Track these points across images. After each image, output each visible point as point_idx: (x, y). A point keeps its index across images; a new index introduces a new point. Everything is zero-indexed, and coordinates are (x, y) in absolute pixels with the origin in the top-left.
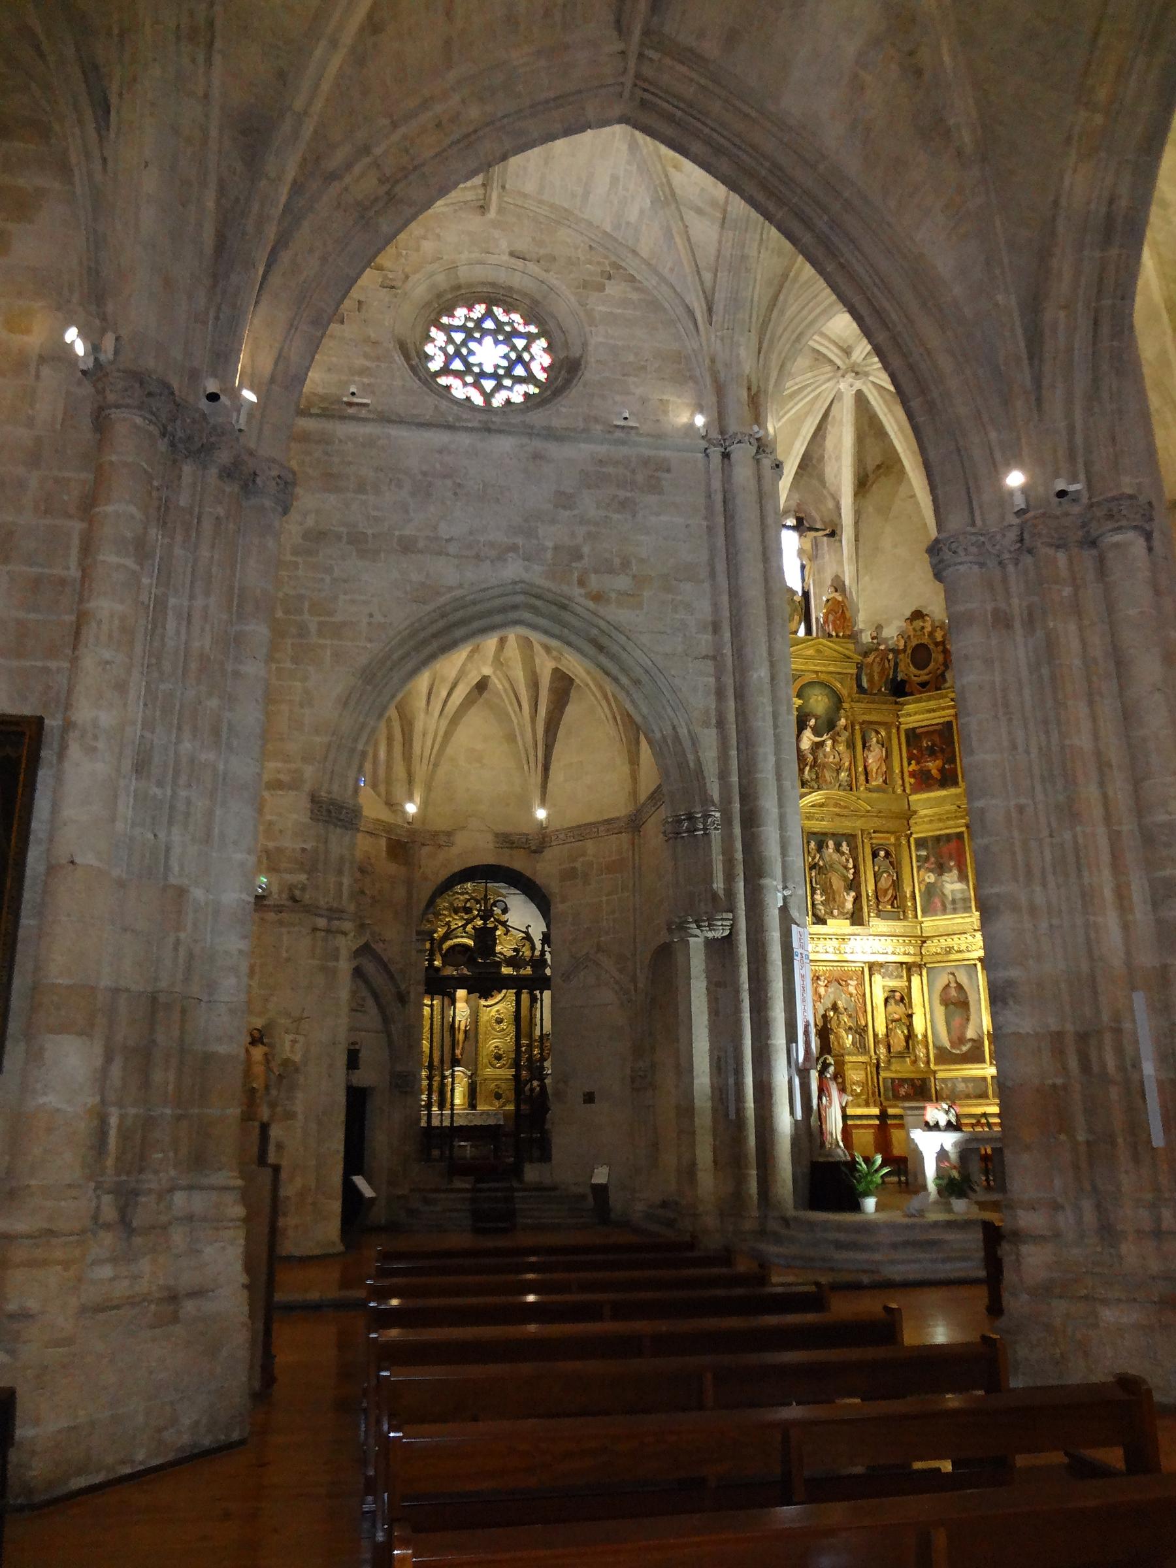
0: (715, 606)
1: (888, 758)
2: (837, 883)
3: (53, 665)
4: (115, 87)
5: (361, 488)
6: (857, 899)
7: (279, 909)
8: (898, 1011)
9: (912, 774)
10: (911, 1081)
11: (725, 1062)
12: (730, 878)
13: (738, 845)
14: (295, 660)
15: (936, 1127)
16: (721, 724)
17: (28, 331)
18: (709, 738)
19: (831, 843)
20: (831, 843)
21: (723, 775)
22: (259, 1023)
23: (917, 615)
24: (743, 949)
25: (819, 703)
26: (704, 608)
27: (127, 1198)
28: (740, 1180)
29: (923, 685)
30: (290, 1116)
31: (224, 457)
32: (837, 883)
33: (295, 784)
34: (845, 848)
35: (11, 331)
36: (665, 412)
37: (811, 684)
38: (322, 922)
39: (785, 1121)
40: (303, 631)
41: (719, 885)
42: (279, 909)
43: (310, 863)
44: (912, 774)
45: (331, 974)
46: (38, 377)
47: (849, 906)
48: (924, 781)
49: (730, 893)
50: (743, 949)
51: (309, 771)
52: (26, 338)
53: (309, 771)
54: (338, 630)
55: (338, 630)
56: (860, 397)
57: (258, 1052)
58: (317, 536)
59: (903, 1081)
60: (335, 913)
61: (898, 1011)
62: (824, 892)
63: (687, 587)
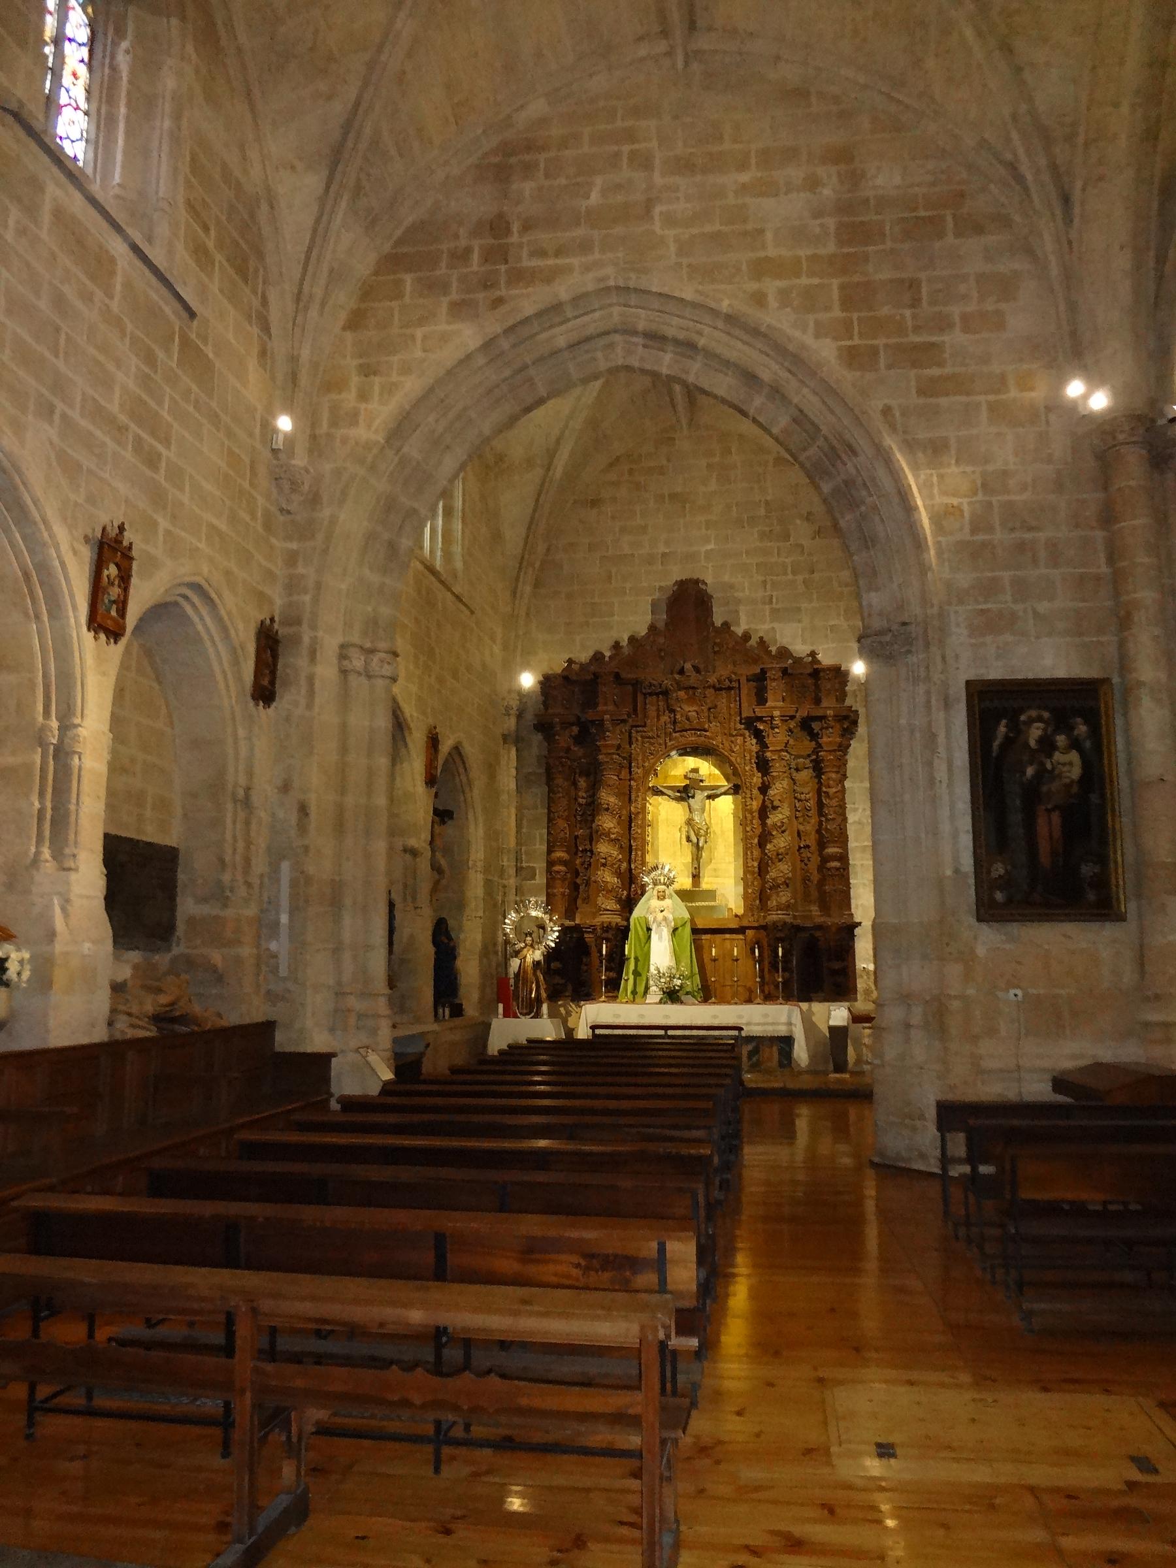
3: (1104, 639)
4: (1079, 184)
17: (1032, 389)
35: (1022, 391)
46: (1047, 422)
52: (1033, 394)
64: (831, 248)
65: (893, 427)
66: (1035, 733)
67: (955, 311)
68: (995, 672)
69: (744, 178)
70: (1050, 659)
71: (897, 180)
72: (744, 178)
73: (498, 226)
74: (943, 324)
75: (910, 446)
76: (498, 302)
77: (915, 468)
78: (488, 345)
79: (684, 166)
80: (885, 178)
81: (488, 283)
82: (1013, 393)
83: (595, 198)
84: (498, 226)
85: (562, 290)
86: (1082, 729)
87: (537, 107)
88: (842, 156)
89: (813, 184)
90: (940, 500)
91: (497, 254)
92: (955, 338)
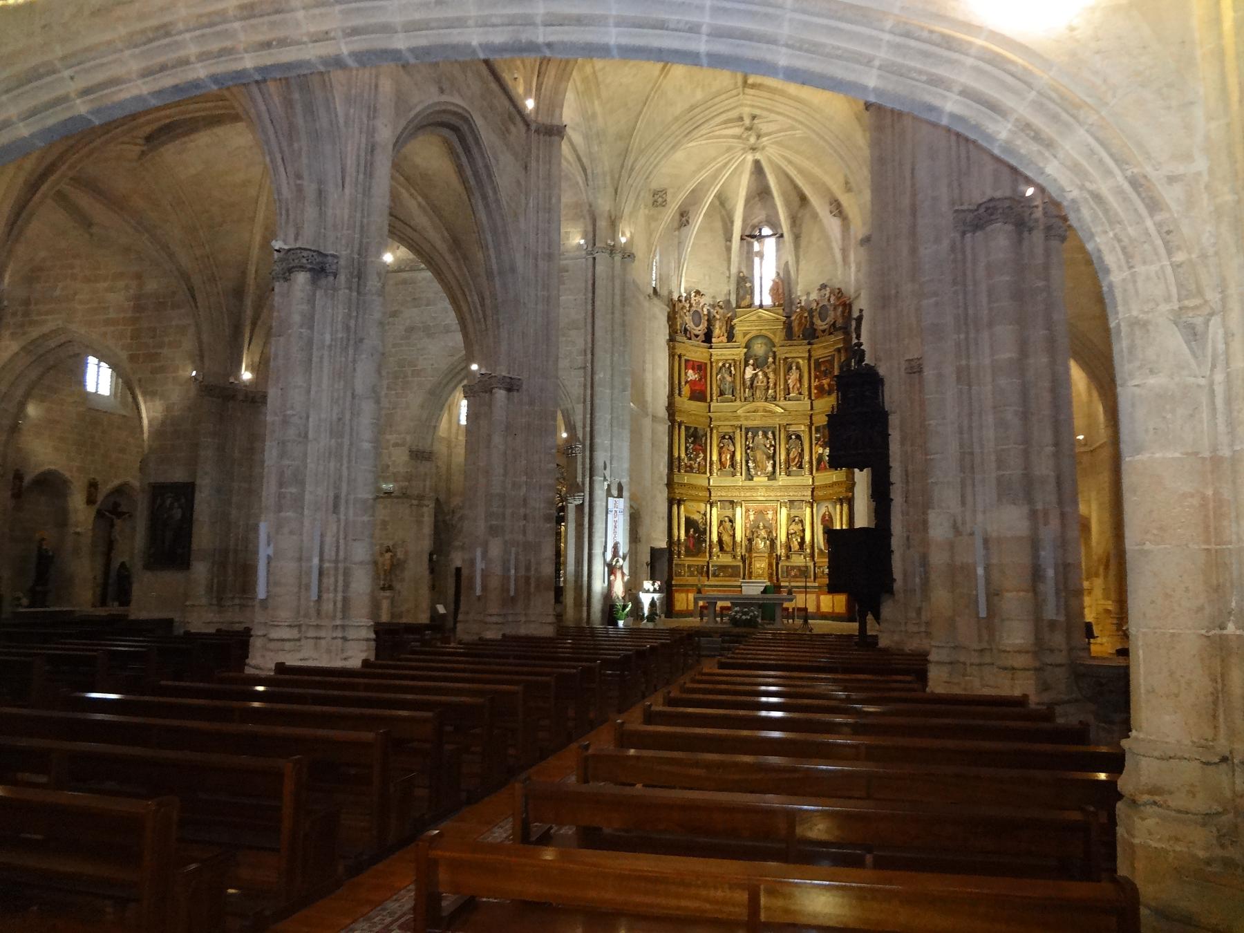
0: (586, 344)
1: (800, 380)
2: (760, 456)
5: (427, 305)
6: (774, 466)
7: (397, 497)
8: (795, 528)
9: (816, 388)
10: (799, 568)
11: (579, 562)
12: (584, 476)
13: (588, 461)
14: (403, 389)
15: (648, 591)
16: (584, 402)
18: (579, 408)
19: (760, 433)
20: (760, 433)
21: (584, 427)
22: (390, 544)
23: (823, 287)
24: (587, 510)
25: (759, 349)
26: (580, 344)
27: (220, 599)
28: (581, 612)
29: (824, 331)
30: (403, 580)
31: (241, 398)
32: (760, 456)
33: (403, 445)
34: (770, 435)
36: (568, 239)
37: (757, 337)
38: (415, 502)
39: (598, 586)
40: (406, 377)
41: (579, 480)
42: (397, 497)
43: (409, 478)
44: (816, 388)
45: (419, 523)
47: (770, 469)
48: (822, 391)
49: (583, 484)
50: (587, 510)
51: (408, 438)
53: (408, 438)
54: (417, 373)
55: (417, 373)
56: (757, 165)
57: (388, 555)
58: (411, 330)
59: (793, 568)
60: (421, 498)
61: (795, 528)
62: (754, 461)
63: (573, 333)
64: (129, 315)
65: (140, 387)
66: (168, 502)
67: (166, 340)
68: (161, 480)
69: (106, 285)
70: (178, 475)
71: (156, 286)
72: (106, 285)
73: (27, 302)
74: (161, 345)
75: (144, 394)
76: (24, 334)
77: (145, 402)
78: (23, 348)
79: (87, 280)
80: (152, 286)
81: (22, 325)
82: (181, 372)
83: (58, 293)
84: (27, 302)
85: (46, 329)
86: (183, 500)
87: (43, 254)
88: (138, 276)
89: (127, 287)
90: (152, 414)
91: (26, 314)
92: (165, 351)
